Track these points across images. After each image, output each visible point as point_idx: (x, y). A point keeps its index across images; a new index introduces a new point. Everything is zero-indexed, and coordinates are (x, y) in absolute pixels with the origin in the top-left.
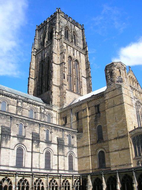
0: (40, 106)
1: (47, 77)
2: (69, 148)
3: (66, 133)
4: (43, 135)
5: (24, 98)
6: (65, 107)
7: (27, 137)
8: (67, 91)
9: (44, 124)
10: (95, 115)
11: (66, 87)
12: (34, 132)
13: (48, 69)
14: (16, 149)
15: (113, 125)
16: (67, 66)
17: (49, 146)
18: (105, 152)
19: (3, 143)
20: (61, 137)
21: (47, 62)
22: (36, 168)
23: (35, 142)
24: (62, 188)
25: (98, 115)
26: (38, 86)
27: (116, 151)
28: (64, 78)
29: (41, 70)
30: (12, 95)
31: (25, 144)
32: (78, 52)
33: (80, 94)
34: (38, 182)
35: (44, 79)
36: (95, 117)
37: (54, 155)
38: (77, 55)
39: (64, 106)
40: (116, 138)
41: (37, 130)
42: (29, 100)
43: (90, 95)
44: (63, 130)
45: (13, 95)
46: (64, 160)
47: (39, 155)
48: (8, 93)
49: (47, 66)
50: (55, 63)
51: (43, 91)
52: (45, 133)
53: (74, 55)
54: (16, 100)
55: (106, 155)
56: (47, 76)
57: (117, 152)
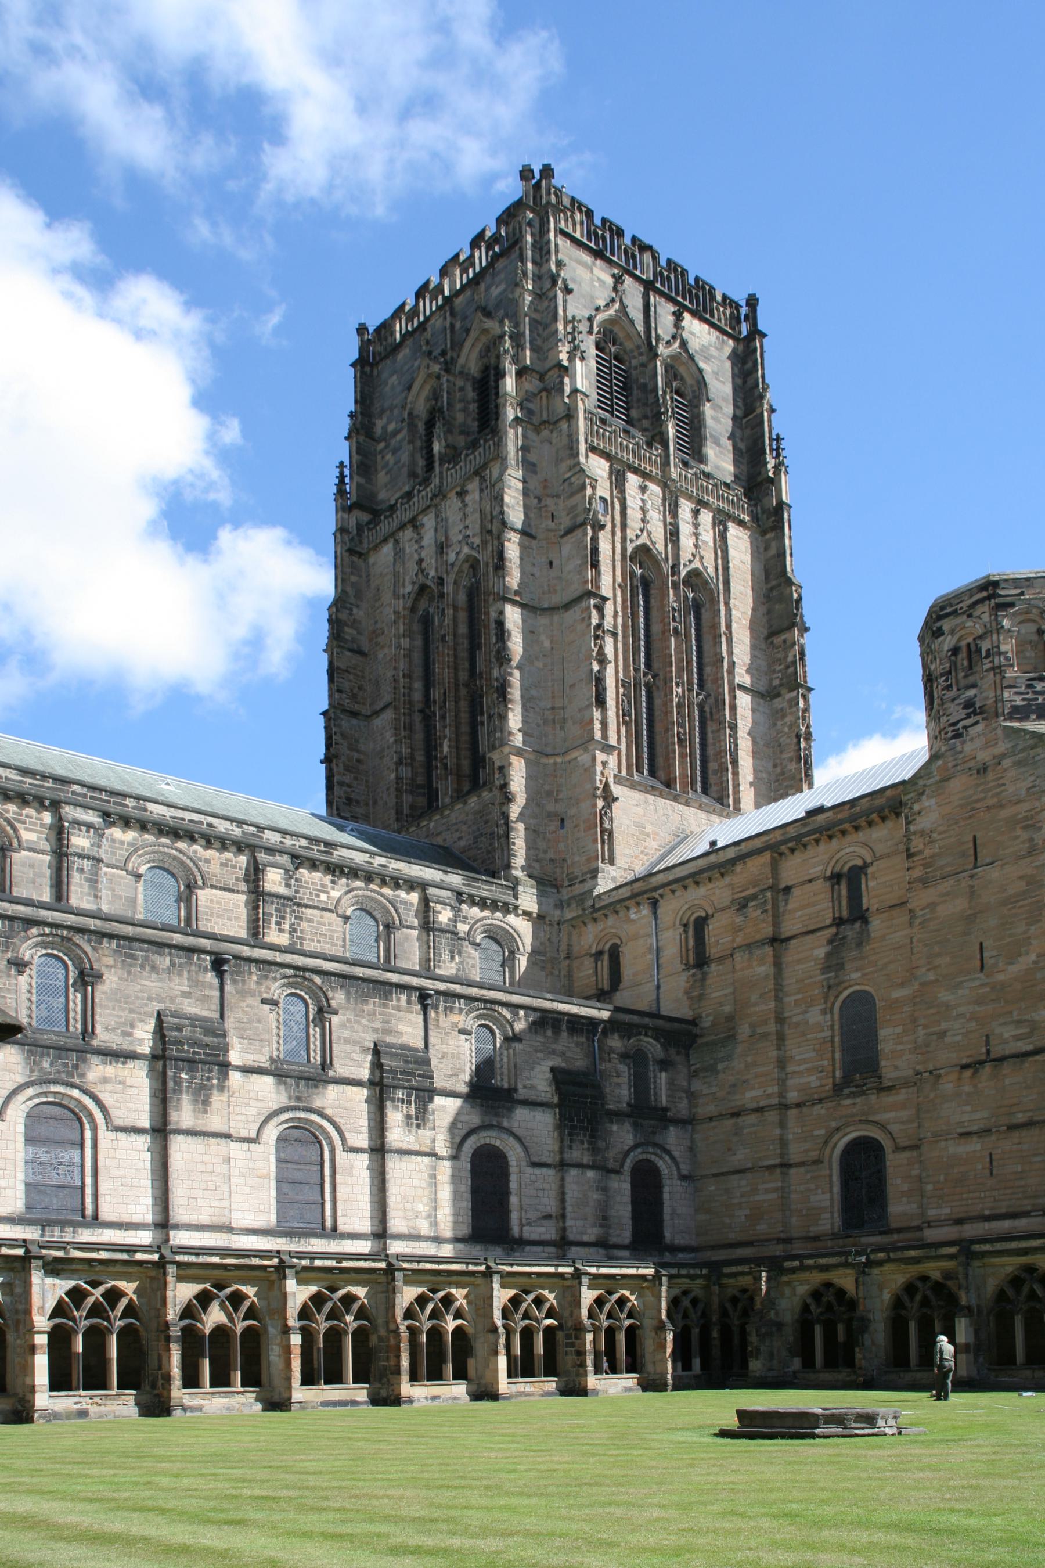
1: (464, 705)
8: (616, 790)
9: (460, 996)
11: (612, 760)
12: (389, 1039)
13: (474, 645)
14: (272, 1133)
16: (620, 620)
17: (497, 1115)
18: (887, 1144)
19: (178, 1108)
20: (580, 1063)
22: (418, 1238)
23: (400, 1094)
24: (589, 1337)
29: (417, 657)
30: (210, 825)
31: (329, 1112)
39: (600, 881)
40: (974, 1066)
45: (222, 826)
47: (434, 1168)
48: (180, 814)
54: (243, 859)
55: (895, 1162)
56: (463, 691)
57: (975, 1146)
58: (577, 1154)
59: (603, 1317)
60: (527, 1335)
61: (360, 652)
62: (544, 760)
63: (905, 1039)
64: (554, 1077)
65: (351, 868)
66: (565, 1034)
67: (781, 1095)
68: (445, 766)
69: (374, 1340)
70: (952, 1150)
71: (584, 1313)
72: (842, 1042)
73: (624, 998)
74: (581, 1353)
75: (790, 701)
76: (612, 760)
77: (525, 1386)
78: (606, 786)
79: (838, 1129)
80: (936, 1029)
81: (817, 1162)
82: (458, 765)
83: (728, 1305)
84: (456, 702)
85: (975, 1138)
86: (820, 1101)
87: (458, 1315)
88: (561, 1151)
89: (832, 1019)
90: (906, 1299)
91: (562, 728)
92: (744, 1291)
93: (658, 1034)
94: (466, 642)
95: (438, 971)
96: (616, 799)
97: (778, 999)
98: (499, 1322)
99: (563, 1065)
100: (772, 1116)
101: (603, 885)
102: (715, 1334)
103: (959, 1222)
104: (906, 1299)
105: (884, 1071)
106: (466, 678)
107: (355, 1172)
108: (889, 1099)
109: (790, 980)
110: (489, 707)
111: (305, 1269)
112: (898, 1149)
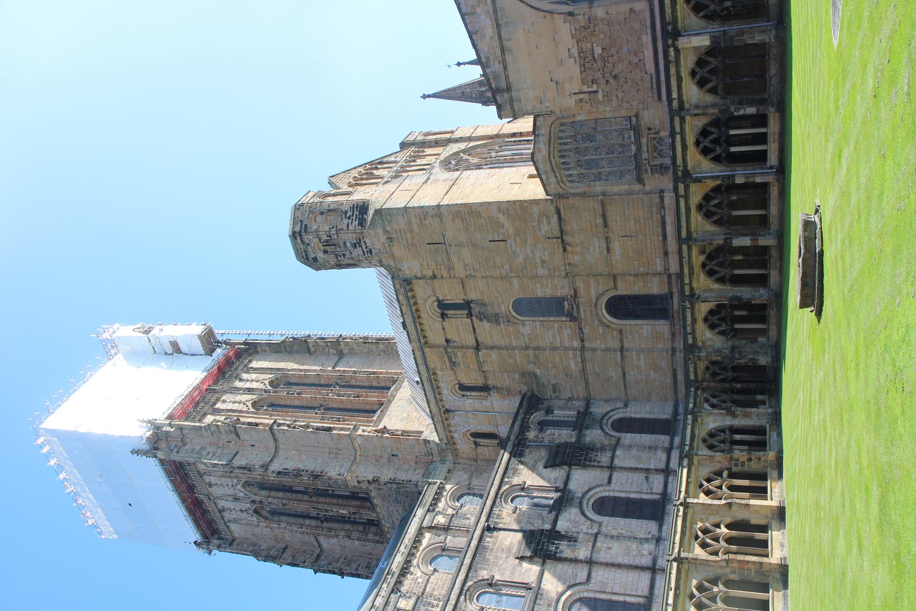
1: (321, 500)
3: (531, 435)
6: (434, 437)
8: (381, 426)
10: (474, 318)
15: (514, 253)
17: (572, 499)
21: (264, 493)
25: (476, 309)
27: (608, 249)
29: (292, 520)
35: (327, 511)
36: (481, 320)
37: (610, 481)
44: (518, 444)
46: (630, 447)
47: (606, 536)
49: (281, 494)
50: (271, 461)
56: (314, 499)
62: (358, 461)
63: (545, 283)
64: (550, 466)
65: (404, 563)
70: (618, 257)
75: (345, 346)
78: (376, 431)
84: (319, 503)
85: (611, 245)
89: (529, 321)
91: (341, 450)
94: (287, 494)
96: (385, 427)
99: (543, 461)
105: (564, 294)
106: (307, 496)
107: (605, 580)
108: (582, 292)
109: (504, 342)
110: (324, 486)
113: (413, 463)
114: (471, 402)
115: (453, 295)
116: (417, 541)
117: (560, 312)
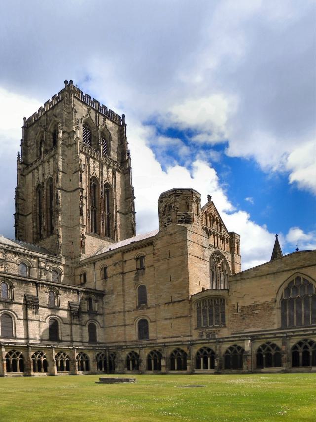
0: (35, 257)
1: (49, 214)
2: (89, 315)
4: (44, 297)
5: (8, 246)
7: (16, 300)
8: (86, 236)
9: (45, 284)
11: (85, 229)
13: (51, 200)
25: (140, 272)
26: (33, 227)
28: (82, 214)
29: (38, 201)
31: (13, 310)
32: (110, 170)
33: (113, 239)
34: (38, 355)
35: (44, 217)
36: (136, 274)
38: (108, 174)
40: (169, 303)
41: (33, 291)
42: (18, 249)
43: (128, 242)
49: (49, 195)
51: (44, 237)
52: (47, 296)
53: (102, 174)
56: (49, 211)
57: (168, 321)
58: (75, 321)
59: (80, 358)
60: (62, 362)
61: (23, 200)
66: (71, 294)
67: (124, 309)
68: (44, 228)
69: (25, 362)
70: (163, 322)
71: (75, 357)
72: (138, 297)
73: (87, 286)
74: (75, 366)
76: (85, 229)
77: (62, 373)
78: (83, 235)
79: (137, 317)
80: (159, 294)
81: (133, 324)
82: (48, 228)
83: (111, 356)
86: (133, 310)
87: (45, 357)
88: (71, 320)
90: (151, 355)
92: (114, 353)
93: (95, 294)
95: (42, 278)
97: (123, 287)
98: (55, 359)
100: (122, 314)
101: (82, 259)
102: (107, 362)
103: (164, 338)
104: (151, 355)
108: (148, 310)
109: (126, 282)
111: (7, 346)
112: (151, 322)
113: (69, 251)
114: (99, 273)
115: (147, 262)
116: (31, 256)
117: (140, 303)
